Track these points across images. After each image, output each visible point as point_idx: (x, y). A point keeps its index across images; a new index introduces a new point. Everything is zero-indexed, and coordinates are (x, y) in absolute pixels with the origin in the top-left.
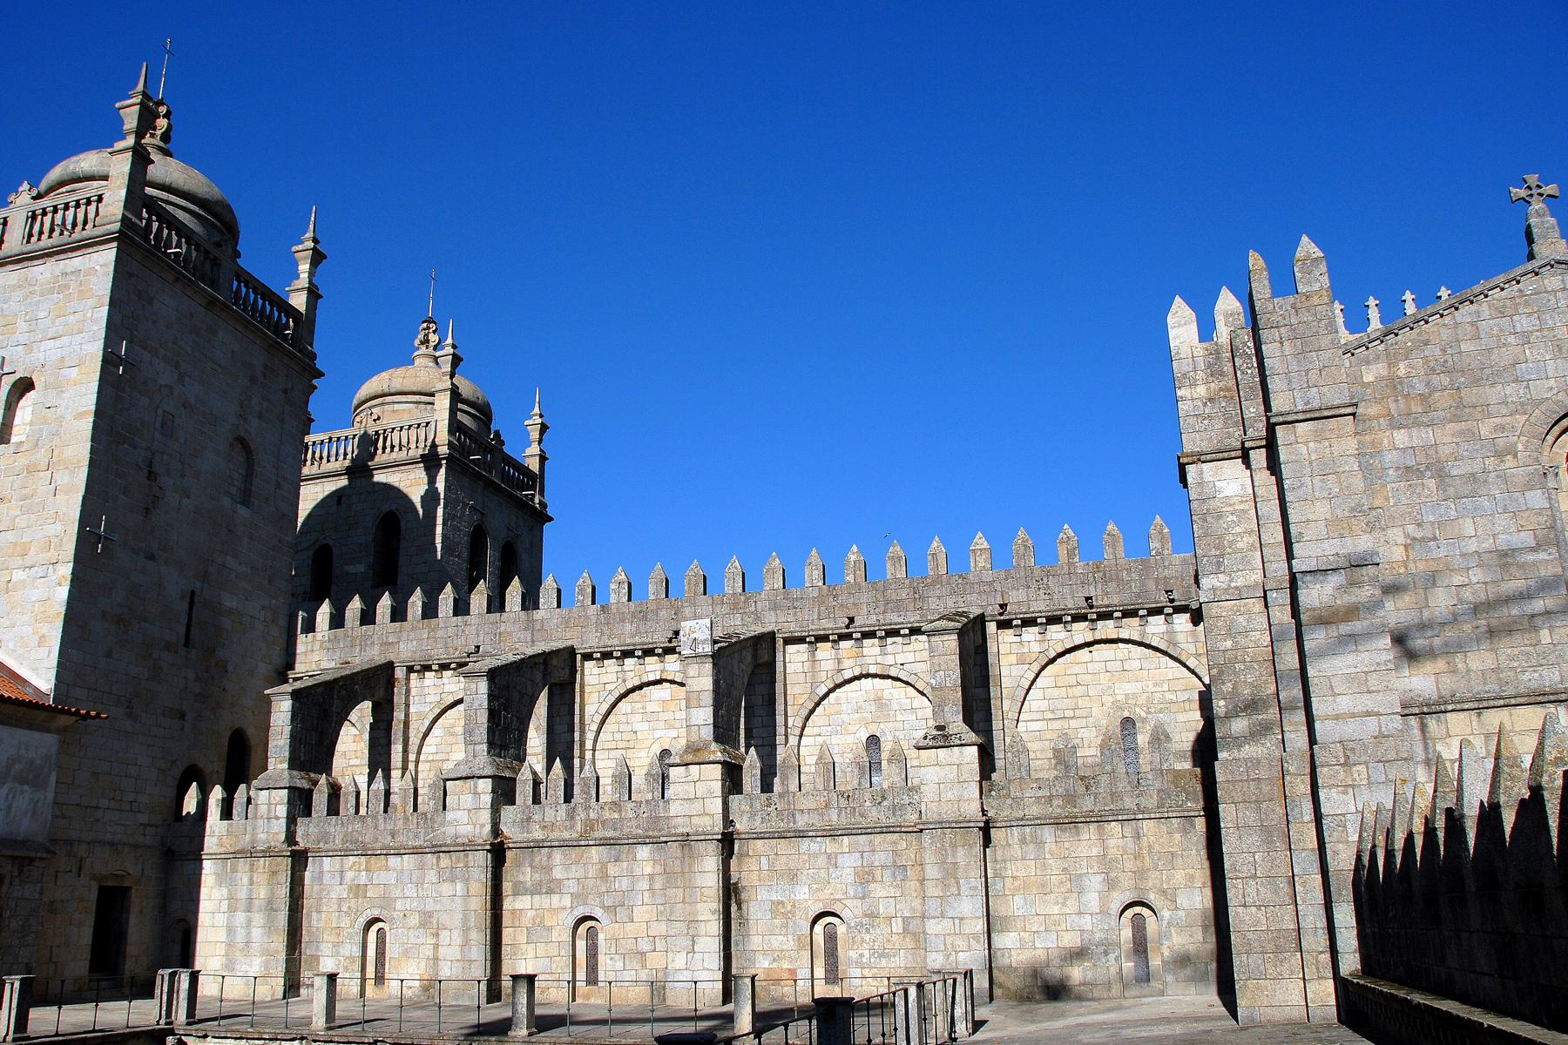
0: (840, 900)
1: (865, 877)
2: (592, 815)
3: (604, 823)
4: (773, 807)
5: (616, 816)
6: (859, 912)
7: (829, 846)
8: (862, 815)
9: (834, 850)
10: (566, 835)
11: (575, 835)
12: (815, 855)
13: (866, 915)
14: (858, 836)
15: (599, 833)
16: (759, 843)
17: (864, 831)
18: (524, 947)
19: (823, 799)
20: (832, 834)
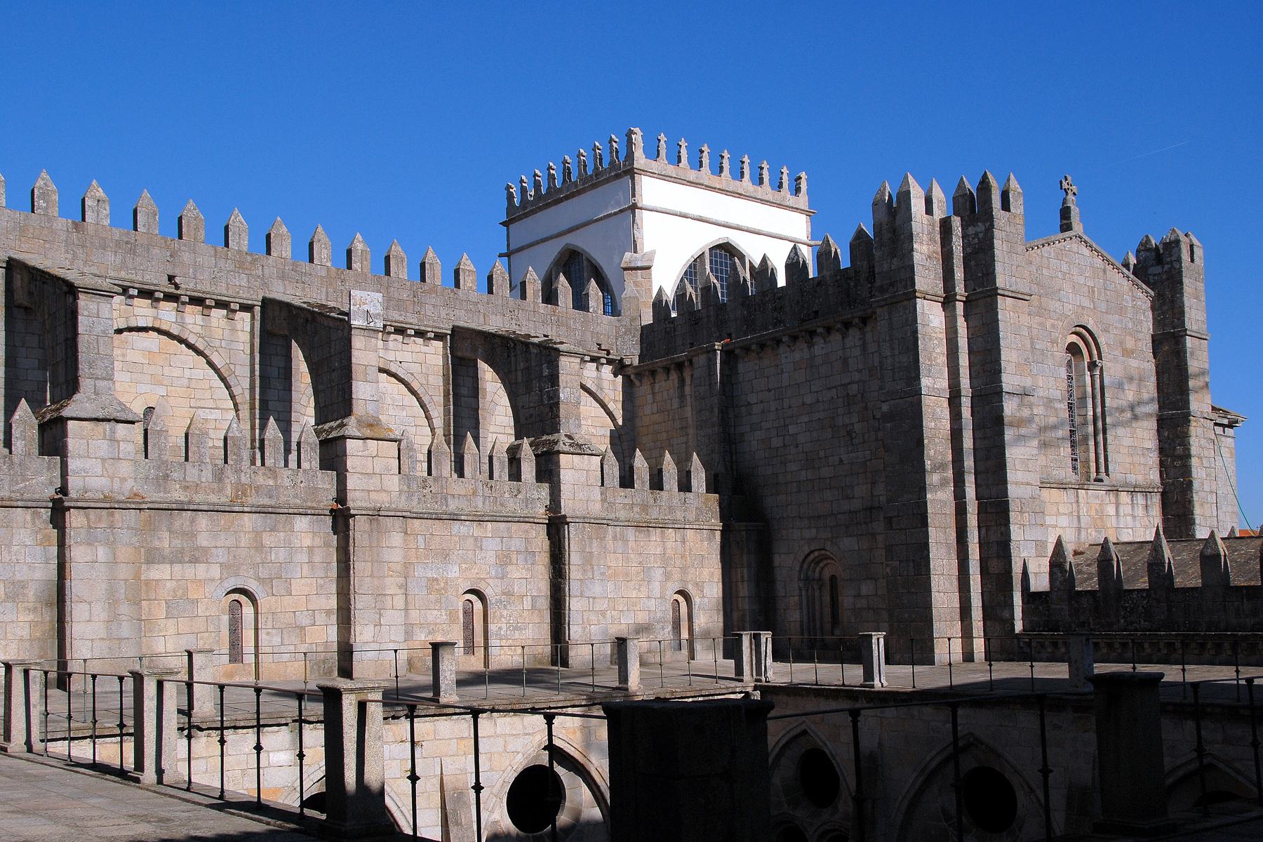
0: (484, 579)
1: (504, 560)
2: (244, 479)
3: (258, 488)
4: (428, 490)
5: (271, 482)
6: (498, 590)
7: (476, 530)
8: (502, 505)
9: (480, 534)
10: (213, 498)
11: (224, 500)
12: (465, 538)
13: (504, 594)
14: (499, 523)
15: (253, 500)
16: (417, 522)
17: (506, 519)
18: (162, 623)
19: (471, 487)
20: (480, 520)
